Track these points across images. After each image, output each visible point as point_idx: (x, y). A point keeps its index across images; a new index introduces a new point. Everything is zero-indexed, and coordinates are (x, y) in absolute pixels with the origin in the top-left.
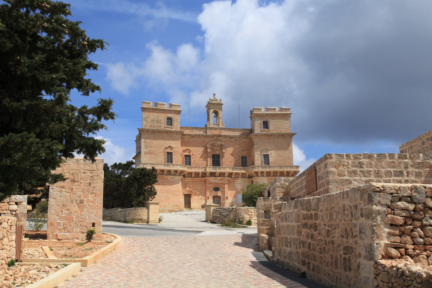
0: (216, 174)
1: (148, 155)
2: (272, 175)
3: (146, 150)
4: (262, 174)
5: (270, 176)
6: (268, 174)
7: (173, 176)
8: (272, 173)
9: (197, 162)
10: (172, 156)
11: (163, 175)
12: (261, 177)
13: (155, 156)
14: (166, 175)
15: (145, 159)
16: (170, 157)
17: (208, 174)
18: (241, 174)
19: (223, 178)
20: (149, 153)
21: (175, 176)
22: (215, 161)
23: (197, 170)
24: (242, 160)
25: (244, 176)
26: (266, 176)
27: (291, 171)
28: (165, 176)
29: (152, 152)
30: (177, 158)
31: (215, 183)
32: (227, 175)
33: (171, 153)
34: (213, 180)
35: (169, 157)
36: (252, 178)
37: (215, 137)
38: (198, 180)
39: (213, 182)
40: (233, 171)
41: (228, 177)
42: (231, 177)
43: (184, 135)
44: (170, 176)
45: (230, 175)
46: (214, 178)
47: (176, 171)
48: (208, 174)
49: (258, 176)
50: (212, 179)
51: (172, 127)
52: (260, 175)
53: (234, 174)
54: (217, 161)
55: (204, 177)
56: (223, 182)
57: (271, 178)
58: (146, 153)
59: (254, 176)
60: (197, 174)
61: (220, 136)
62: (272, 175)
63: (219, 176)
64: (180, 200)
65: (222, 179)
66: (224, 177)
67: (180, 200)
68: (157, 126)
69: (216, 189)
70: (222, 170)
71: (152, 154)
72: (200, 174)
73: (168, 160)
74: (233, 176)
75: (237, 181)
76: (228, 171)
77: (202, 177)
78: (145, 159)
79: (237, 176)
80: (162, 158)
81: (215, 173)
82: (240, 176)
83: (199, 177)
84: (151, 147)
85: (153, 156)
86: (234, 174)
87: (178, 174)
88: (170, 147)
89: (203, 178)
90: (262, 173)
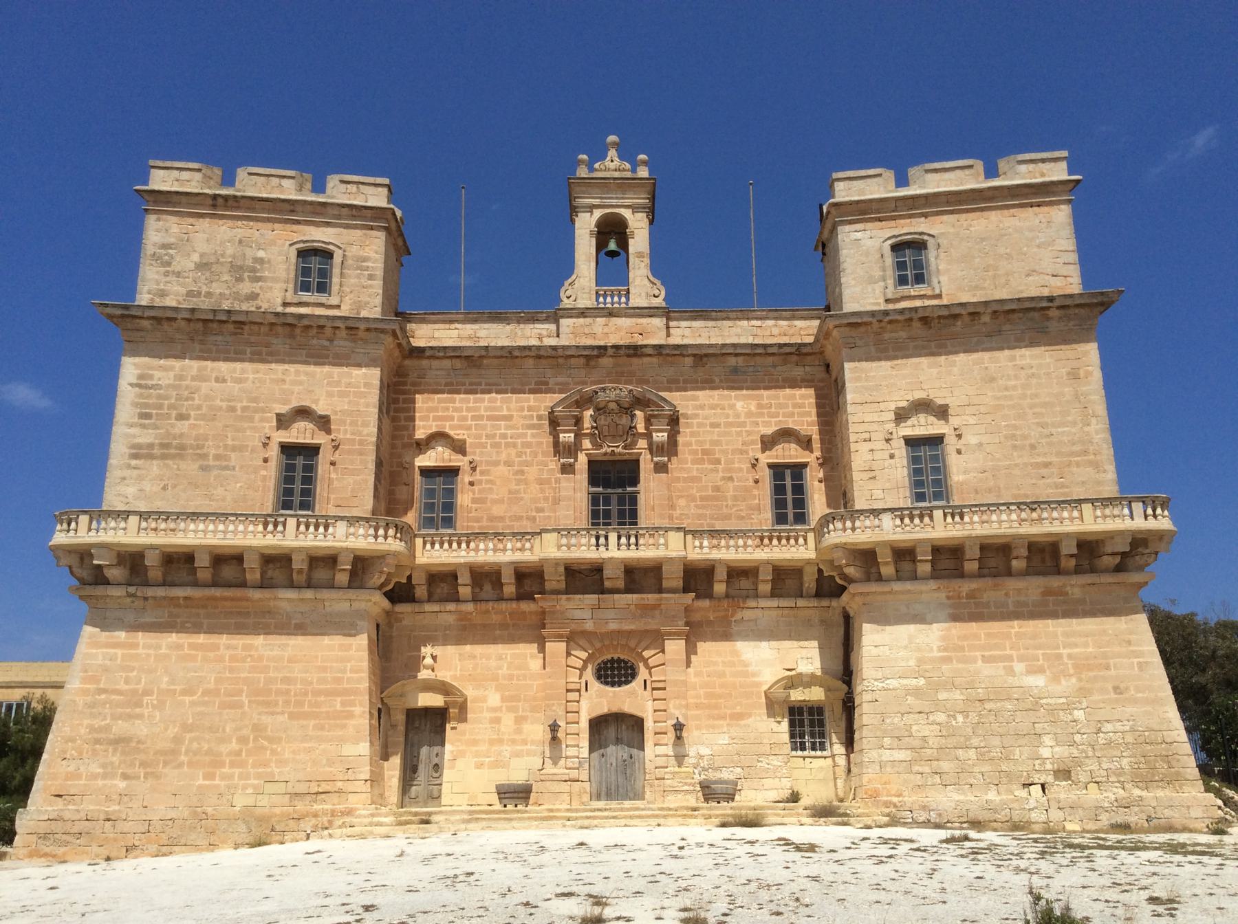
0: (607, 573)
1: (155, 467)
2: (971, 566)
3: (146, 437)
4: (906, 566)
5: (961, 575)
6: (946, 563)
7: (309, 594)
8: (973, 552)
9: (497, 510)
10: (310, 468)
11: (243, 584)
12: (897, 586)
13: (204, 468)
14: (264, 585)
15: (131, 490)
16: (298, 473)
17: (555, 580)
18: (766, 575)
19: (651, 598)
20: (169, 450)
21: (325, 594)
22: (607, 501)
23: (485, 554)
24: (779, 490)
25: (790, 583)
26: (936, 575)
27: (1112, 535)
28: (256, 594)
29: (182, 447)
30: (350, 479)
31: (602, 636)
32: (673, 578)
33: (311, 451)
34: (587, 614)
35: (299, 474)
36: (845, 597)
37: (606, 361)
38: (495, 618)
39: (589, 626)
40: (716, 555)
41: (686, 590)
42: (708, 594)
43: (419, 352)
44: (291, 594)
45: (697, 578)
46: (591, 599)
47: (325, 561)
48: (555, 580)
49: (880, 579)
50: (580, 608)
51: (334, 300)
52: (887, 570)
53: (721, 574)
54: (621, 500)
55: (529, 597)
56: (652, 624)
57: (966, 586)
58: (140, 453)
59: (851, 580)
60: (485, 577)
61: (635, 351)
62: (971, 566)
63: (628, 590)
64: (349, 750)
65: (646, 609)
66: (660, 590)
67: (349, 750)
68: (236, 296)
69: (615, 672)
70: (646, 552)
71: (182, 457)
72: (508, 578)
73: (288, 492)
74: (719, 588)
75: (747, 614)
76: (670, 548)
77: (520, 597)
78: (131, 490)
79: (745, 584)
80: (260, 481)
81: (597, 569)
82: (765, 588)
83: (501, 599)
84: (182, 417)
85: (190, 467)
86: (721, 574)
87: (342, 578)
88: (303, 413)
89: (526, 606)
90: (904, 554)
